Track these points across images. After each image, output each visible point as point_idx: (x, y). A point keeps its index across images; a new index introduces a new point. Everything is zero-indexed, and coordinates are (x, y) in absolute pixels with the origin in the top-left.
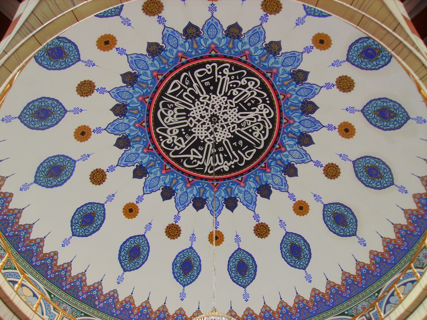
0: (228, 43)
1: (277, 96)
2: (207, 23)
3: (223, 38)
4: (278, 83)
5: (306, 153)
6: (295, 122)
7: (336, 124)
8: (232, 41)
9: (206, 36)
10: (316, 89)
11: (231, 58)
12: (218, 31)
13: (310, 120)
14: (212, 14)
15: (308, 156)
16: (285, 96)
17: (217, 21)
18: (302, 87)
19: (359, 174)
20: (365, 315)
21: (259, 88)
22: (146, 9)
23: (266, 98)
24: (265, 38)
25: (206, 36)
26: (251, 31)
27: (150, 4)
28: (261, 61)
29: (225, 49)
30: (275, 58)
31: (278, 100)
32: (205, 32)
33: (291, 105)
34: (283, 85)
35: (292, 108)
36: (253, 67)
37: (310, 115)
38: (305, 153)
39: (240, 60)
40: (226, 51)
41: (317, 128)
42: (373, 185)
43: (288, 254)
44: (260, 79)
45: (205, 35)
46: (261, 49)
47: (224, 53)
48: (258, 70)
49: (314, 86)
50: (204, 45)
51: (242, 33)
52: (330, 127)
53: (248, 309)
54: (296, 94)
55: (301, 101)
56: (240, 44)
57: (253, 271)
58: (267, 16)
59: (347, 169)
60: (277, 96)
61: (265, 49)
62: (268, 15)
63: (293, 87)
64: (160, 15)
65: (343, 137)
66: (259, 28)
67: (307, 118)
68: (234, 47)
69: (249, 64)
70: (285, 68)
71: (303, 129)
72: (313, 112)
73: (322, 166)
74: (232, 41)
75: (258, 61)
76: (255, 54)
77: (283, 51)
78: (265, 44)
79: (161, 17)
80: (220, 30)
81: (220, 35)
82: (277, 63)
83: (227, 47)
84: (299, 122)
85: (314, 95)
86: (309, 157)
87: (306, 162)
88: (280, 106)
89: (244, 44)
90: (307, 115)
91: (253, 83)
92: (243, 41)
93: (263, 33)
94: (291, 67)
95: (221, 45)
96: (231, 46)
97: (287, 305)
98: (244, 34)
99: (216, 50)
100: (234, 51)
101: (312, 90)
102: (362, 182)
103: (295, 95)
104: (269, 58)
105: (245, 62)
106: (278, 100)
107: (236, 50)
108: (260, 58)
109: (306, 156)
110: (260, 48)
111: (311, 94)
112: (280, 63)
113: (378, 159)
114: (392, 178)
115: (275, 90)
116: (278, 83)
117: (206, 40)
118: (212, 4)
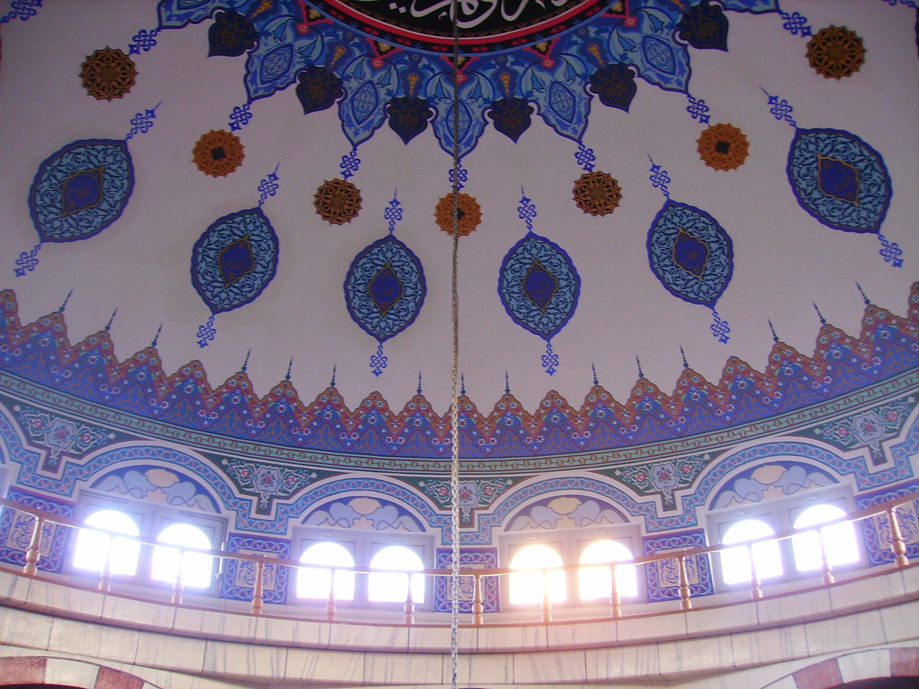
0: (605, 52)
1: (394, 37)
2: (687, 69)
3: (624, 57)
4: (425, 61)
5: (190, 21)
6: (298, 36)
7: (244, 135)
8: (601, 61)
9: (665, 35)
10: (356, 133)
11: (568, 23)
12: (649, 66)
13: (282, 75)
14: (689, 96)
15: (179, 23)
16: (381, 53)
17: (668, 86)
18: (381, 106)
19: (82, 150)
21: (444, 14)
22: (852, 46)
23: (408, 9)
24: (548, 122)
25: (665, 35)
26: (583, 113)
27: (848, 62)
28: (504, 69)
29: (597, 33)
30: (486, 100)
31: (383, 33)
32: (673, 44)
33: (350, 53)
34: (413, 67)
35: (340, 52)
36: (507, 44)
37: (298, 82)
38: (192, 18)
39: (545, 33)
40: (592, 31)
41: (254, 82)
42: (46, 185)
44: (464, 32)
45: (670, 37)
46: (530, 93)
47: (593, 24)
48: (491, 46)
49: (367, 133)
50: (650, 11)
51: (596, 96)
52: (241, 116)
54: (370, 82)
55: (345, 82)
56: (579, 68)
58: (585, 169)
59: (107, 119)
60: (394, 37)
61: (525, 101)
62: (587, 172)
63: (393, 86)
64: (808, 39)
65: (204, 137)
66: (575, 131)
67: (293, 70)
68: (583, 51)
69: (519, 40)
70: (448, 101)
71: (267, 45)
72: (300, 92)
73: (133, 50)
74: (601, 61)
75: (508, 65)
76: (529, 72)
77: (490, 128)
78: (532, 109)
79: (804, 35)
80: (647, 69)
81: (636, 57)
82: (473, 96)
83: (599, 42)
84: (290, 46)
85: (345, 122)
86: (173, 23)
87: (163, 9)
88: (362, 25)
89: (571, 74)
90: (300, 74)
91: (468, 12)
92: (578, 80)
93: (559, 128)
94: (443, 114)
95: (614, 35)
96: (594, 50)
98: (592, 97)
99: (618, 17)
100: (576, 43)
101: (359, 123)
102: (58, 155)
103: (368, 77)
104: (498, 92)
105: (530, 37)
106: (383, 33)
107: (574, 50)
108: (514, 74)
109: (180, 18)
110: (535, 93)
111: (351, 114)
112: (469, 101)
113: (120, 213)
114: (62, 240)
115: (413, 42)
116: (425, 61)
117: (657, 26)
118: (706, 121)
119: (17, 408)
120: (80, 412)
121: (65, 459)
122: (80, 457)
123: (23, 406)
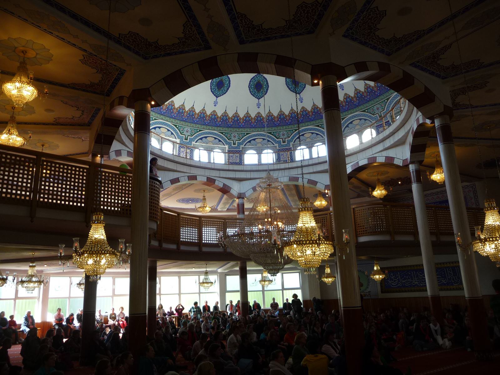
20: (282, 139)
43: (252, 87)
53: (214, 111)
57: (226, 89)
97: (239, 116)
119: (366, 111)
120: (377, 102)
121: (382, 113)
122: (384, 110)
123: (367, 109)
